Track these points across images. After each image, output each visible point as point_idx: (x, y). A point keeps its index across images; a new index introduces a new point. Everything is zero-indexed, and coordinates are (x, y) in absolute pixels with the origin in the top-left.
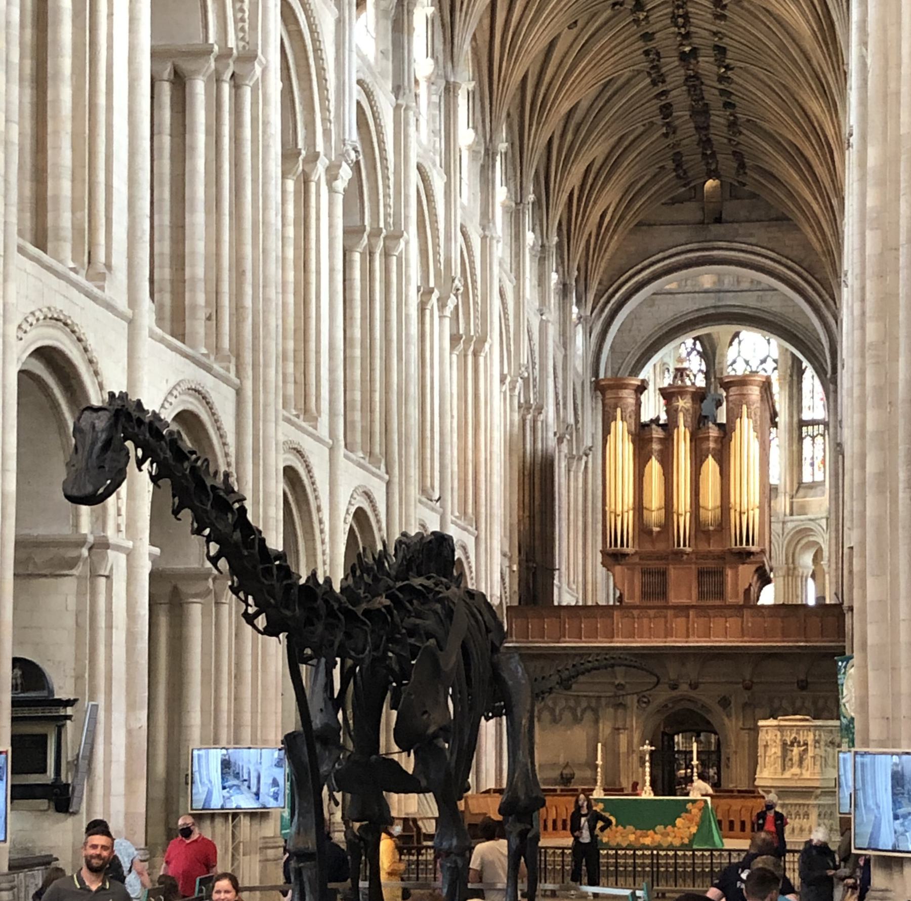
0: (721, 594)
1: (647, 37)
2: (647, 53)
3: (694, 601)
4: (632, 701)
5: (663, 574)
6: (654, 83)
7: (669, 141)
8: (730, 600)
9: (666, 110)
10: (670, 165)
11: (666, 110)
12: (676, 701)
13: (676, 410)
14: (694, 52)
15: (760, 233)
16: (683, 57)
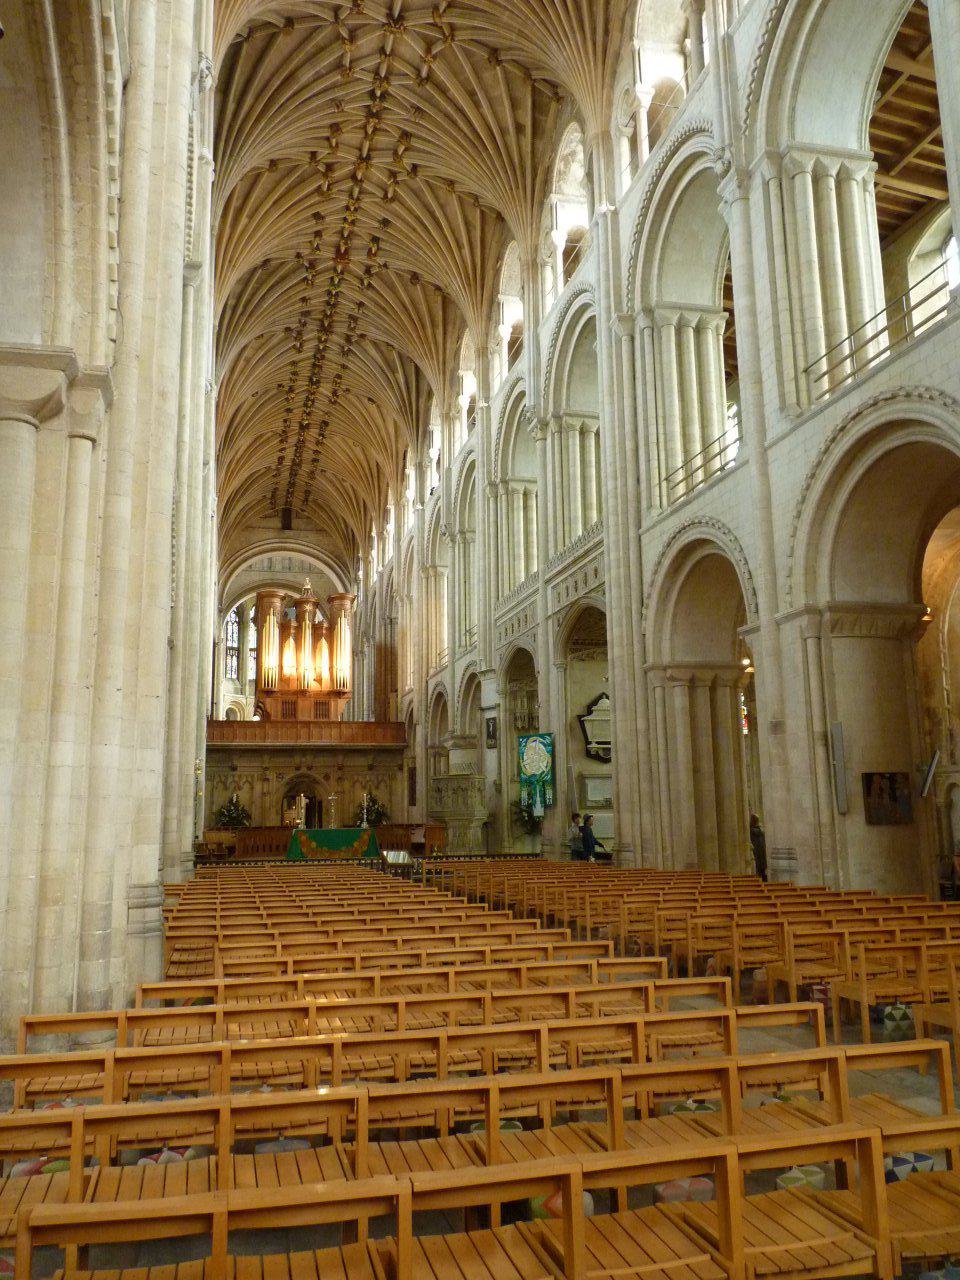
0: (327, 715)
1: (289, 411)
2: (285, 421)
3: (312, 719)
4: (271, 775)
5: (295, 704)
6: (282, 441)
7: (275, 480)
8: (333, 718)
9: (281, 459)
10: (269, 495)
11: (281, 459)
12: (298, 777)
13: (305, 612)
14: (308, 425)
15: (313, 537)
16: (303, 428)
